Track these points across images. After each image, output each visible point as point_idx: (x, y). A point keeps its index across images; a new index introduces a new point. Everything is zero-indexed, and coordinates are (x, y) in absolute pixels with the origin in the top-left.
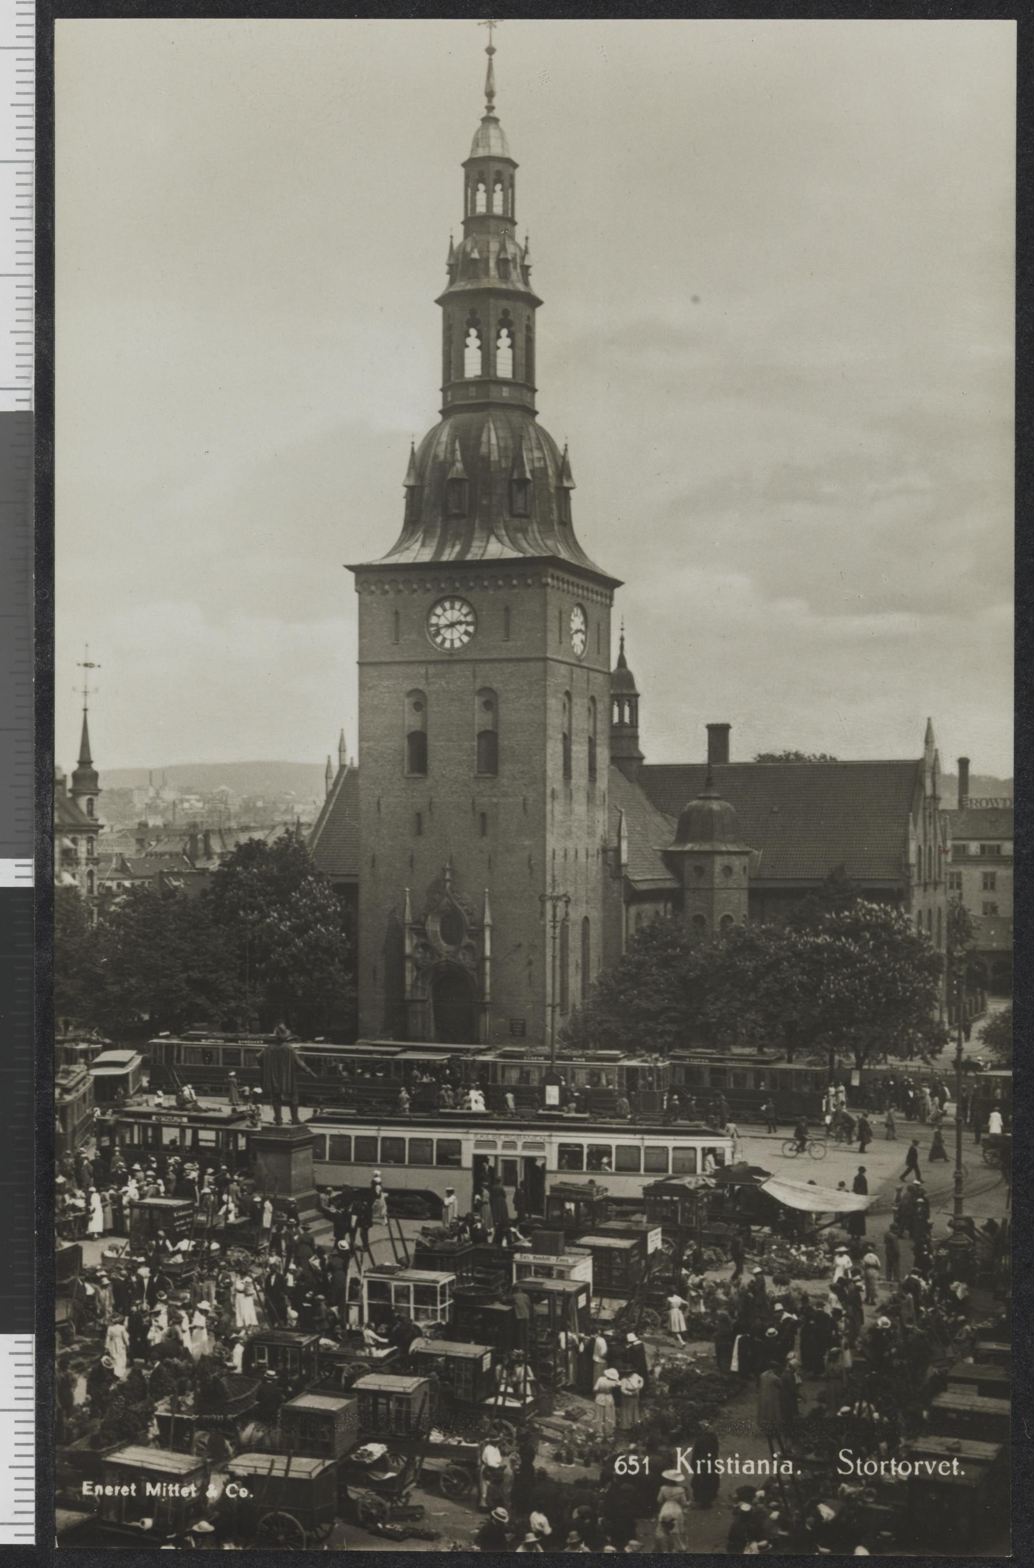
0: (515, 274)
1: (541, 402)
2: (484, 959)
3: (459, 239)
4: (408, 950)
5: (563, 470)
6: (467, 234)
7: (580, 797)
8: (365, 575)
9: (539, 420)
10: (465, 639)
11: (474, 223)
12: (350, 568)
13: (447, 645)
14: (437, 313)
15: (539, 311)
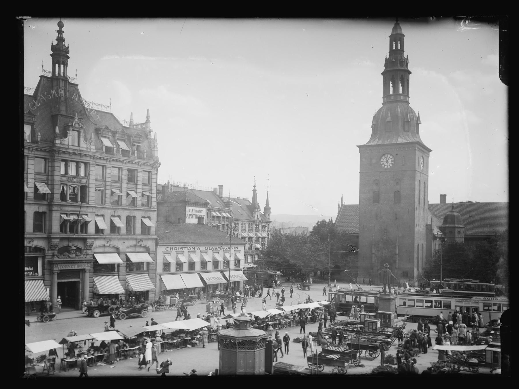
0: (405, 65)
1: (410, 100)
3: (388, 57)
4: (373, 252)
5: (418, 119)
6: (390, 55)
7: (422, 211)
8: (361, 148)
9: (410, 105)
10: (391, 165)
12: (358, 146)
13: (386, 167)
14: (382, 76)
15: (410, 75)
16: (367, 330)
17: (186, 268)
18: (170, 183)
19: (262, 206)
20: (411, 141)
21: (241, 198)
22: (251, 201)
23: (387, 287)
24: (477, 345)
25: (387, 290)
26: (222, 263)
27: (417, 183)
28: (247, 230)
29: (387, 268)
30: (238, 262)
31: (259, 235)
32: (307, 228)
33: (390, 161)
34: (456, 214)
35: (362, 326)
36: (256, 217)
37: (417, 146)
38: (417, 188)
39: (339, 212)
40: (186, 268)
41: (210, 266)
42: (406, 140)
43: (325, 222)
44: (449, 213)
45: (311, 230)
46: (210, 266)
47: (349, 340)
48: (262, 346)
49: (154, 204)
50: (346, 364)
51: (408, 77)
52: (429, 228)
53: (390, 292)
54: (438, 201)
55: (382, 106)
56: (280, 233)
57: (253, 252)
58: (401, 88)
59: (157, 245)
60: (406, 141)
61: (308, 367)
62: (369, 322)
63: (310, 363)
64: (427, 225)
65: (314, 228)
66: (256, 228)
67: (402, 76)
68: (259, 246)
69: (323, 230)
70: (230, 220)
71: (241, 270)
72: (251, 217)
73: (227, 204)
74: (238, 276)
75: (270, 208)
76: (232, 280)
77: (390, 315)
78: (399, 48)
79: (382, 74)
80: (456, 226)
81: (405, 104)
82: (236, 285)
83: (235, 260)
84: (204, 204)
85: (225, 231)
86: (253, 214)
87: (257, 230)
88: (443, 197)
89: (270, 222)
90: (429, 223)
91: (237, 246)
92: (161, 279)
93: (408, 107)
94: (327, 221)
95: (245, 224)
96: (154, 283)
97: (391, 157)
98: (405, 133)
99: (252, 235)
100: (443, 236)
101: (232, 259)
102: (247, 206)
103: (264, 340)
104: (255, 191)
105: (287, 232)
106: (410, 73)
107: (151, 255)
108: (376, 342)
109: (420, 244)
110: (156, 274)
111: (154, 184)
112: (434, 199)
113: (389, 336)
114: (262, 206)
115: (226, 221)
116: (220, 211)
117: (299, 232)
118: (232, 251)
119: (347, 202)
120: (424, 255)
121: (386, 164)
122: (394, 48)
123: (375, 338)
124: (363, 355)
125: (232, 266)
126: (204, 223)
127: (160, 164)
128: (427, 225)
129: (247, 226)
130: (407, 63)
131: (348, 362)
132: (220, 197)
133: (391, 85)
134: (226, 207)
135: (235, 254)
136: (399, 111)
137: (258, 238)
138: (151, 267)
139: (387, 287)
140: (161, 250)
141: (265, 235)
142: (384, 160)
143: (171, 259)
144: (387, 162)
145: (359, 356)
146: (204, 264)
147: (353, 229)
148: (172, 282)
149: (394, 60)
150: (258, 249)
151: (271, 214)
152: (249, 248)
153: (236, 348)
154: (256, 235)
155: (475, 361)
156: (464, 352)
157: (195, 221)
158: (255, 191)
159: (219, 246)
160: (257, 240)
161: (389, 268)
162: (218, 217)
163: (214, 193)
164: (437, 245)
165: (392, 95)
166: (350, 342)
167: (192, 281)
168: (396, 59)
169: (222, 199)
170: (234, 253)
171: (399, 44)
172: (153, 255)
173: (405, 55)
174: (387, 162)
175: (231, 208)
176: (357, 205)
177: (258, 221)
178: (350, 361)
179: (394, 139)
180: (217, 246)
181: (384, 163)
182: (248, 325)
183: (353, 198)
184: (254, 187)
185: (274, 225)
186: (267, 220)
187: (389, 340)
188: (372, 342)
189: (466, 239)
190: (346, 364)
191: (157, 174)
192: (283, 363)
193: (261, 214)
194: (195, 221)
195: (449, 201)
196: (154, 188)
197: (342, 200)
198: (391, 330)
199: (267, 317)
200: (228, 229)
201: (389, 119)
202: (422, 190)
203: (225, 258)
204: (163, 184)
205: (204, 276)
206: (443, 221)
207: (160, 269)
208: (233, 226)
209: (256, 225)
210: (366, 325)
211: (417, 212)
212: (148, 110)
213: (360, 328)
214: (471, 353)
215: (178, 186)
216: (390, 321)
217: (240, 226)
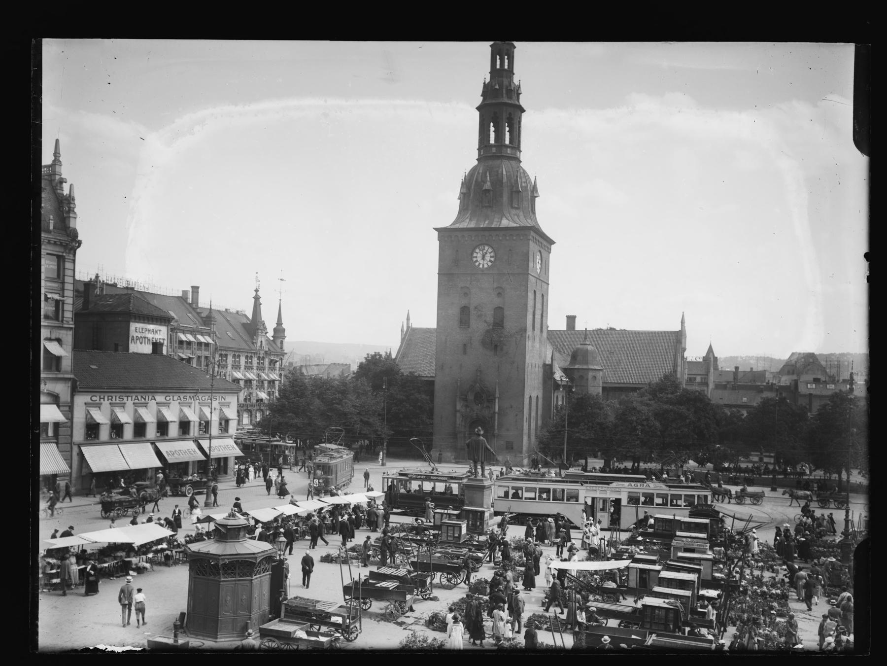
0: (515, 97)
2: (495, 413)
3: (488, 80)
4: (458, 408)
5: (535, 189)
7: (537, 339)
8: (444, 234)
9: (522, 165)
11: (494, 72)
12: (436, 229)
14: (477, 113)
16: (444, 538)
17: (128, 432)
18: (100, 279)
19: (270, 326)
20: (522, 225)
21: (231, 311)
22: (251, 318)
23: (479, 467)
24: (616, 559)
25: (480, 471)
26: (197, 424)
27: (531, 295)
28: (243, 367)
29: (479, 435)
30: (225, 423)
31: (264, 376)
32: (348, 366)
33: (488, 257)
34: (590, 348)
35: (437, 532)
36: (259, 344)
37: (532, 233)
38: (530, 303)
39: (403, 340)
40: (128, 432)
41: (174, 430)
42: (515, 222)
43: (381, 356)
44: (579, 346)
45: (354, 368)
46: (174, 430)
47: (414, 557)
48: (265, 570)
49: (68, 315)
50: (408, 597)
51: (520, 118)
52: (548, 370)
53: (483, 475)
54: (562, 326)
55: (476, 163)
56: (302, 374)
57: (252, 405)
58: (507, 135)
59: (74, 391)
60: (515, 225)
61: (345, 604)
62: (448, 525)
63: (347, 597)
64: (545, 365)
65: (361, 366)
66: (258, 363)
67: (510, 114)
68: (263, 395)
69: (377, 371)
70: (212, 348)
71: (231, 437)
72: (251, 345)
73: (208, 319)
74: (225, 447)
75: (284, 330)
76: (214, 454)
77: (483, 513)
78: (506, 67)
79: (478, 108)
80: (591, 367)
81: (513, 163)
82: (222, 464)
83: (221, 419)
84: (164, 320)
85: (203, 368)
86: (253, 339)
87: (261, 368)
88: (571, 320)
89: (283, 354)
90: (548, 361)
91: (224, 395)
92: (81, 455)
93: (519, 167)
94: (383, 354)
95: (239, 356)
96: (69, 460)
97: (490, 250)
98: (513, 212)
99: (251, 376)
100: (569, 384)
101: (215, 419)
102: (244, 325)
103: (269, 559)
104: (257, 298)
105: (313, 372)
106: (523, 111)
107: (62, 408)
108: (458, 558)
109: (534, 395)
110: (71, 443)
111: (69, 280)
112: (556, 322)
113: (480, 547)
114: (270, 326)
115: (205, 350)
116: (193, 332)
117: (336, 373)
118: (215, 404)
119: (416, 324)
120: (540, 413)
121: (481, 262)
122: (498, 67)
123: (457, 551)
124: (436, 581)
125: (215, 430)
126: (165, 352)
127: (80, 243)
128: (545, 365)
129: (243, 360)
130: (519, 94)
131: (411, 593)
132: (193, 307)
133: (492, 129)
134: (205, 325)
135: (221, 410)
136: (504, 173)
137: (261, 382)
138: (62, 430)
139: (479, 467)
140: (81, 400)
141: (274, 376)
142: (478, 254)
143: (101, 417)
144: (483, 258)
145: (431, 583)
146: (163, 426)
147: (426, 369)
148: (103, 458)
149: (497, 87)
150: (262, 400)
151: (286, 340)
152: (245, 400)
153: (219, 574)
154: (259, 376)
155: (611, 585)
156: (596, 572)
157: (147, 349)
158: (257, 298)
159: (192, 395)
160: (261, 386)
161: (483, 435)
162: (189, 343)
163: (183, 299)
164: (559, 399)
165: (492, 146)
166: (416, 560)
167: (139, 456)
168: (501, 85)
169: (198, 310)
170: (218, 407)
171: (506, 61)
172: (67, 409)
173: (516, 81)
174: (483, 258)
175: (214, 328)
176: (433, 329)
177: (262, 352)
178: (416, 591)
179: (496, 220)
180: (188, 395)
181: (479, 259)
182: (242, 534)
183: (427, 318)
184: (257, 291)
185: (291, 360)
186: (279, 350)
187: (480, 555)
188: (453, 559)
189: (604, 389)
190: (408, 597)
191: (74, 261)
192: (301, 598)
193: (268, 340)
194: (147, 349)
195: (579, 326)
196: (69, 287)
197: (408, 319)
198: (482, 538)
199: (276, 520)
200: (207, 365)
201: (488, 186)
202: (539, 306)
203: (202, 416)
204: (87, 279)
205: (163, 447)
206: (569, 359)
207: (79, 434)
208: (217, 359)
209: (259, 358)
210: (444, 528)
211: (529, 344)
212: (57, 141)
213: (434, 535)
214: (606, 573)
215: (114, 285)
216: (482, 524)
217: (230, 359)
